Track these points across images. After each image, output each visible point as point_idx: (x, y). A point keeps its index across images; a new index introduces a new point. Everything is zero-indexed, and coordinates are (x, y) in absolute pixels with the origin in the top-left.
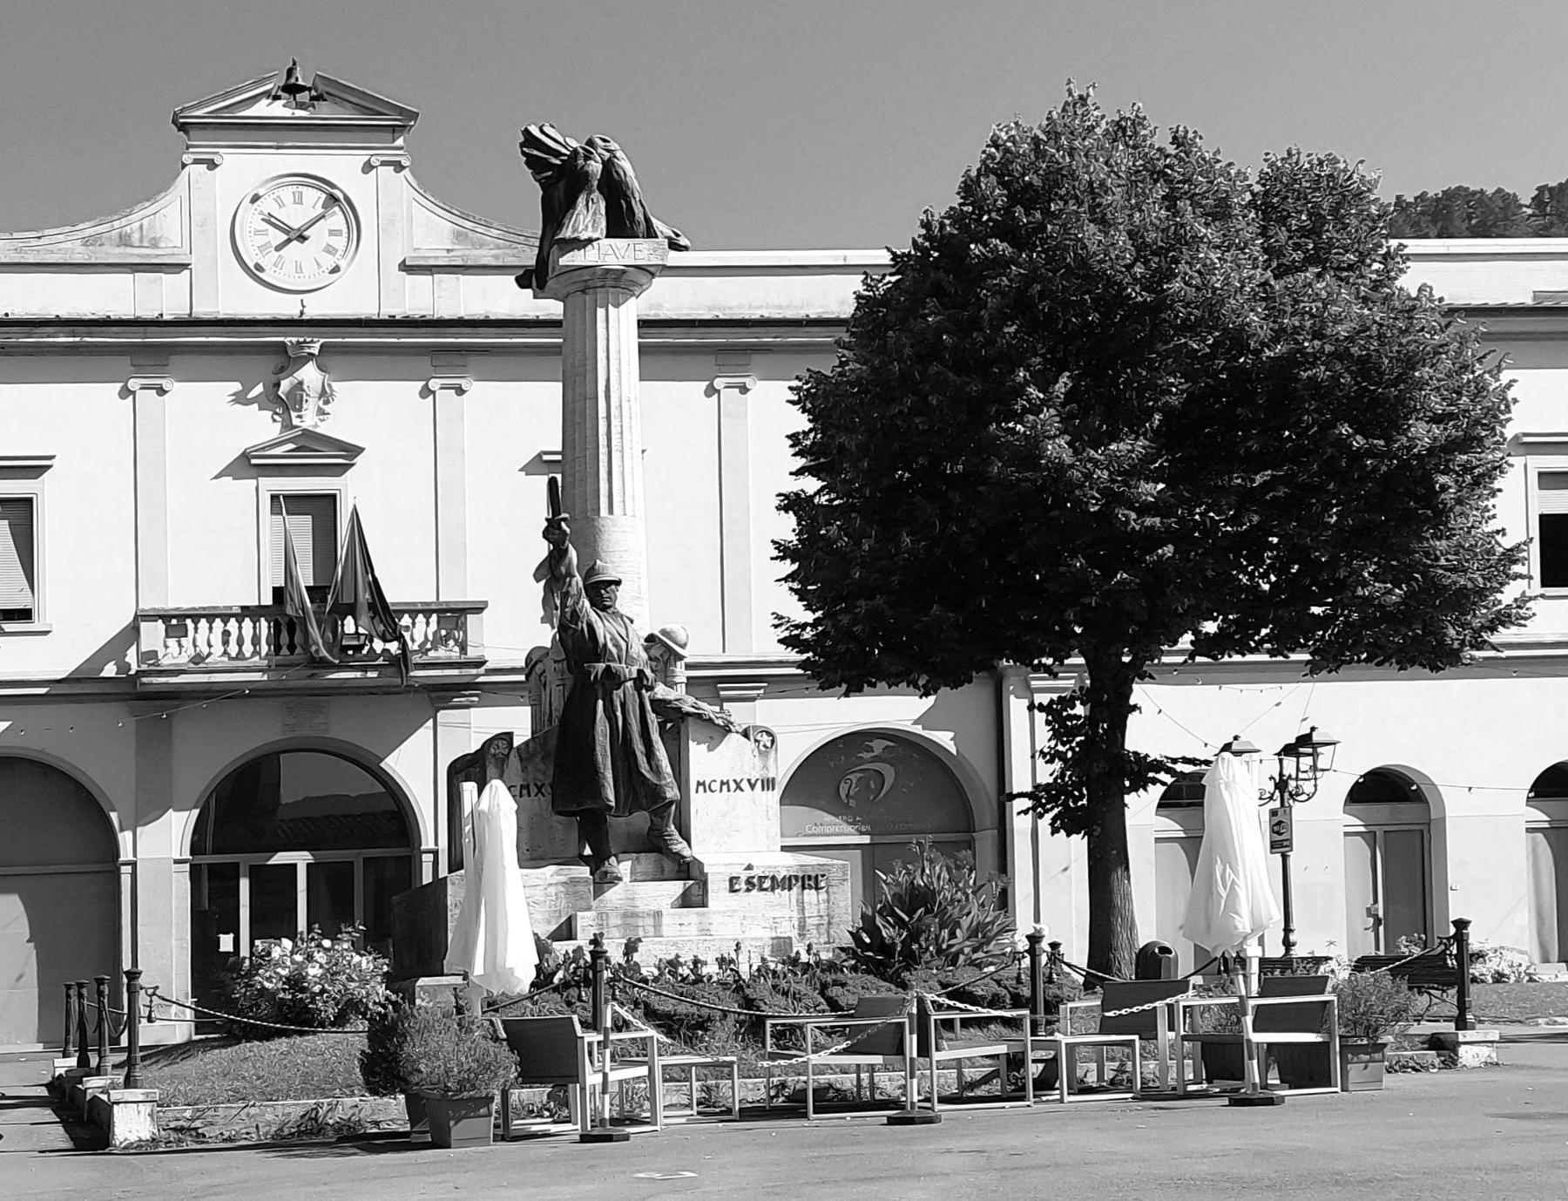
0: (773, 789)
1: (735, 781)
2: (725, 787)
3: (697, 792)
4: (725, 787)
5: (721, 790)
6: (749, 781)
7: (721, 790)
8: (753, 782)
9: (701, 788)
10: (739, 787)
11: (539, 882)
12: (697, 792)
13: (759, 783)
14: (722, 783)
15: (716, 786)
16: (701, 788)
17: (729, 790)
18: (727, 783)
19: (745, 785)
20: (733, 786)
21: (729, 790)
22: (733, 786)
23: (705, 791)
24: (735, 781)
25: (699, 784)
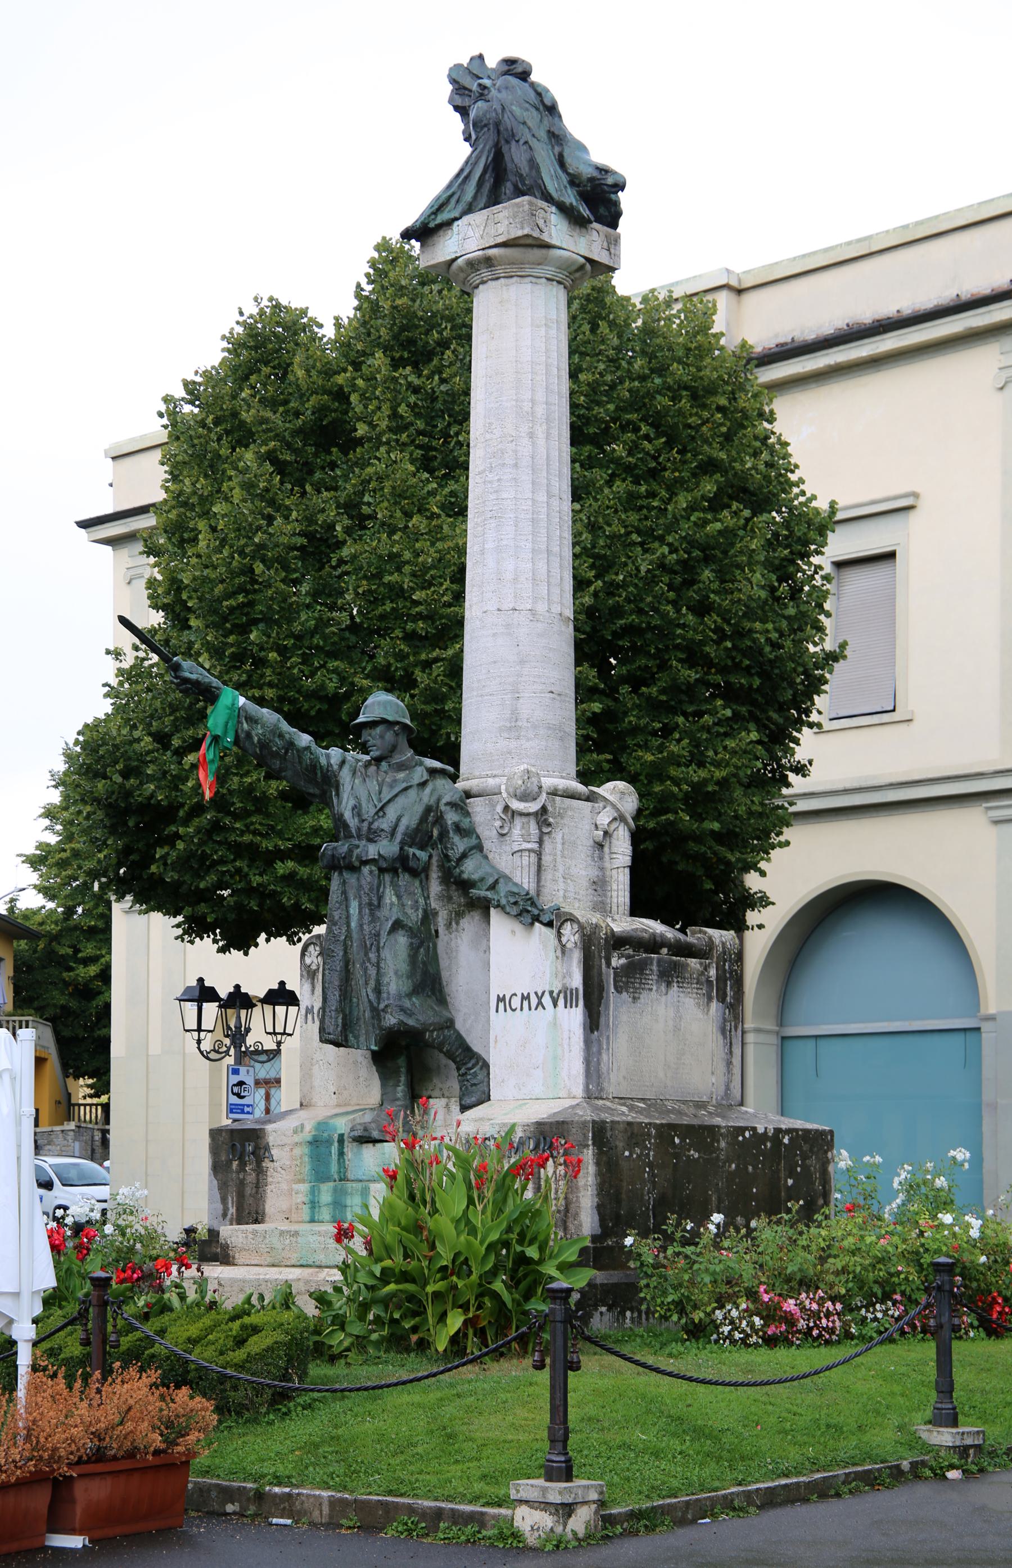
0: (577, 1006)
1: (536, 993)
2: (526, 1003)
3: (497, 1011)
4: (526, 1003)
5: (522, 1009)
6: (551, 993)
7: (522, 1009)
8: (555, 994)
9: (501, 1005)
10: (540, 1003)
11: (286, 1140)
12: (497, 1011)
13: (562, 996)
14: (523, 998)
15: (516, 1002)
16: (501, 1005)
17: (530, 1009)
18: (528, 997)
19: (547, 1000)
20: (534, 1001)
21: (530, 1009)
22: (534, 1001)
23: (505, 1010)
24: (536, 993)
25: (501, 999)
